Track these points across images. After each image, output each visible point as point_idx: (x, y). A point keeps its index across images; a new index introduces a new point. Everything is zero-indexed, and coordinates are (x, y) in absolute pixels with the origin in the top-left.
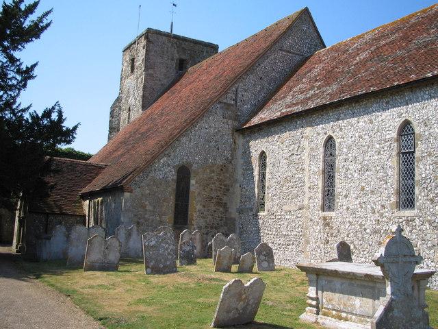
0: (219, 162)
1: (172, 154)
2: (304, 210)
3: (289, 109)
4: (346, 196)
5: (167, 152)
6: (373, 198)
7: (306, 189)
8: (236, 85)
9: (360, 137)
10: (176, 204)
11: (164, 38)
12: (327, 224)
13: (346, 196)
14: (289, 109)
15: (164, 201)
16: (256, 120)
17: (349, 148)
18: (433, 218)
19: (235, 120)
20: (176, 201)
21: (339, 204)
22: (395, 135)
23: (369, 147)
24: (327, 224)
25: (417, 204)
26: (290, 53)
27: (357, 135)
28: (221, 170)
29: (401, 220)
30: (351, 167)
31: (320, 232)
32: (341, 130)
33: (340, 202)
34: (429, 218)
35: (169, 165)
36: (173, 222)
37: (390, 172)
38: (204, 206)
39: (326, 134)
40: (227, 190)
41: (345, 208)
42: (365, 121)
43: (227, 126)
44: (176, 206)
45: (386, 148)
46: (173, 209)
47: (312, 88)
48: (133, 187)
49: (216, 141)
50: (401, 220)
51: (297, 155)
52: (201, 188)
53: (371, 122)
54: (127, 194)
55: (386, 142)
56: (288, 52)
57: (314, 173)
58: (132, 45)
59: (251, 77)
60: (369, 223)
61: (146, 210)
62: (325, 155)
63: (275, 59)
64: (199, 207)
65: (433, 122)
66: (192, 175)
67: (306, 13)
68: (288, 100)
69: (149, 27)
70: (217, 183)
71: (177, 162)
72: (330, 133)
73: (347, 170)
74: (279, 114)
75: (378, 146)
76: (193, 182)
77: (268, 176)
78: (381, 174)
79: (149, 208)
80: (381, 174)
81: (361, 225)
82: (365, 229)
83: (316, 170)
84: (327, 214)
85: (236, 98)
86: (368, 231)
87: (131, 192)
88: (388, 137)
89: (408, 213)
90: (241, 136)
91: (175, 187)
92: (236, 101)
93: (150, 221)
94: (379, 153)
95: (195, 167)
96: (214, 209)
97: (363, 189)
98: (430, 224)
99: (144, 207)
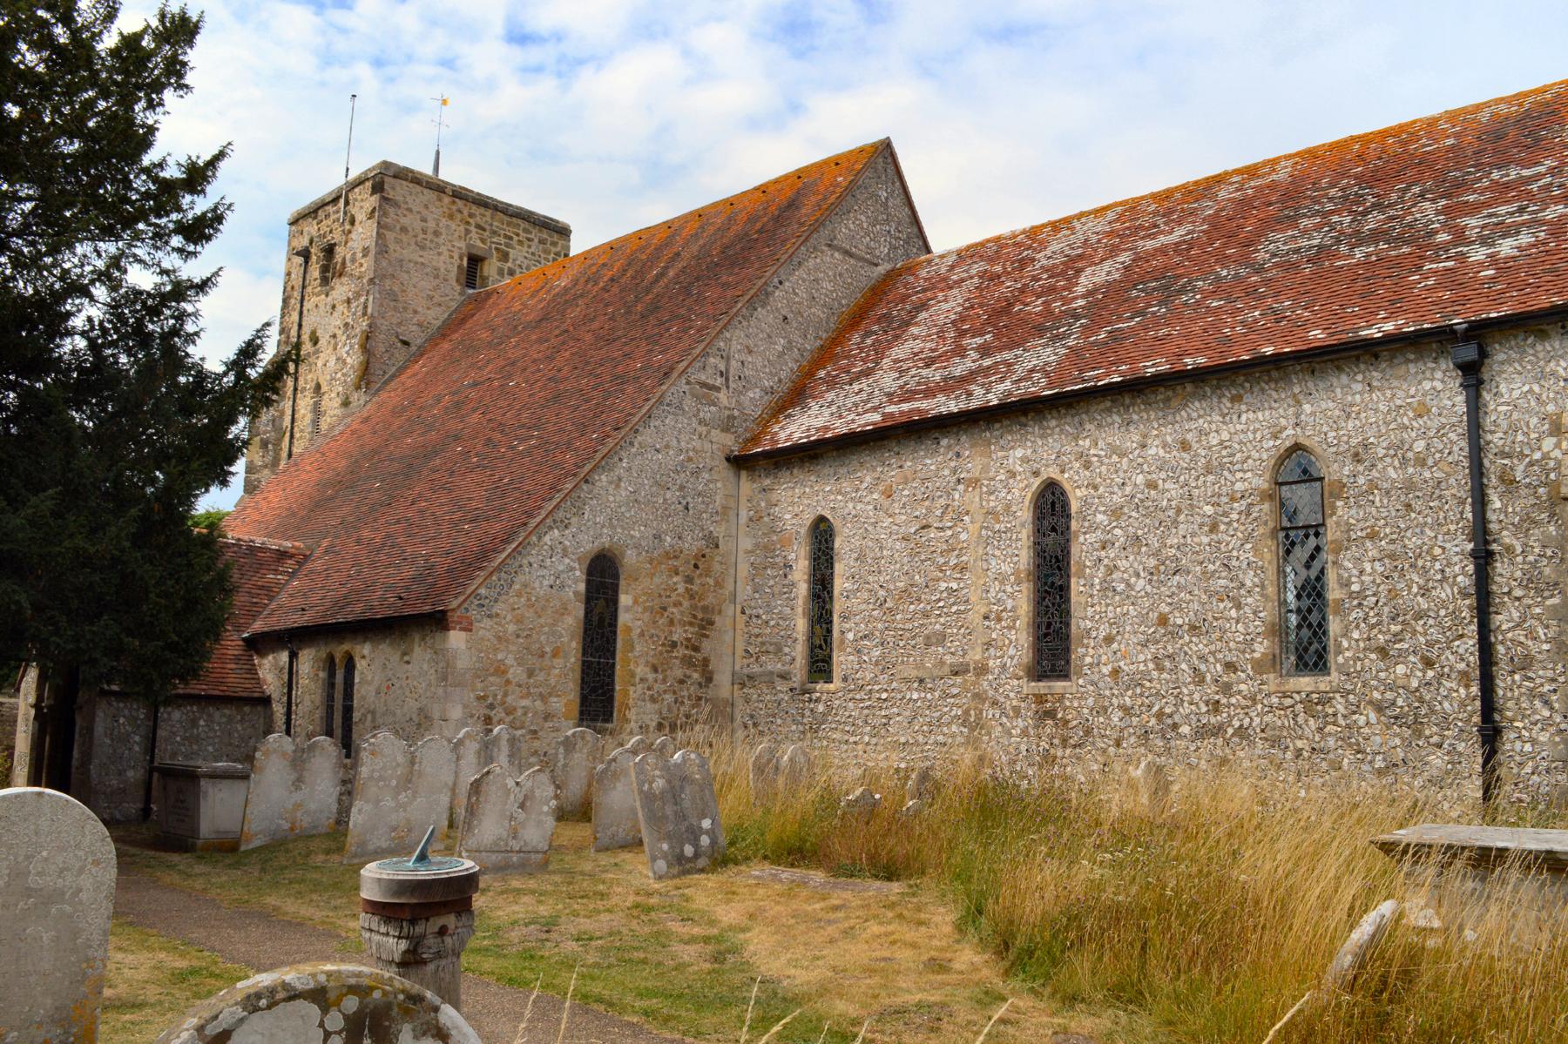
0: (691, 544)
1: (574, 520)
2: (970, 677)
3: (905, 407)
4: (1109, 640)
5: (560, 514)
6: (1200, 646)
7: (974, 618)
9: (1152, 485)
10: (584, 662)
12: (1051, 714)
13: (1109, 640)
14: (905, 407)
15: (555, 654)
16: (796, 429)
17: (1116, 513)
18: (1389, 695)
19: (726, 430)
20: (583, 655)
21: (1088, 660)
22: (1262, 483)
23: (1179, 511)
24: (1051, 714)
25: (1336, 660)
26: (851, 255)
27: (1140, 479)
28: (696, 566)
29: (1288, 702)
30: (1123, 564)
31: (1025, 733)
32: (1087, 465)
33: (1084, 654)
34: (1376, 695)
35: (565, 555)
37: (1249, 579)
38: (655, 670)
39: (1036, 474)
40: (705, 624)
41: (1106, 670)
42: (1165, 445)
43: (707, 446)
44: (586, 668)
45: (1235, 516)
46: (578, 675)
47: (960, 352)
48: (474, 613)
49: (682, 488)
50: (1288, 702)
51: (941, 529)
53: (1185, 446)
54: (456, 639)
55: (1233, 499)
57: (1002, 579)
58: (327, 204)
60: (1186, 709)
61: (508, 682)
62: (1039, 531)
63: (817, 269)
64: (641, 670)
65: (1381, 452)
66: (622, 583)
67: (884, 151)
68: (888, 380)
69: (389, 160)
70: (686, 604)
71: (588, 545)
72: (1053, 473)
73: (1111, 570)
74: (877, 417)
75: (1209, 510)
76: (625, 600)
77: (840, 584)
78: (1222, 582)
79: (516, 673)
80: (1222, 582)
81: (1160, 715)
82: (1175, 726)
83: (1006, 568)
84: (1042, 687)
86: (1185, 729)
88: (1239, 486)
89: (1305, 683)
90: (744, 474)
91: (579, 610)
92: (727, 379)
93: (519, 712)
94: (1214, 528)
95: (630, 558)
97: (1163, 620)
98: (1379, 708)
99: (500, 671)
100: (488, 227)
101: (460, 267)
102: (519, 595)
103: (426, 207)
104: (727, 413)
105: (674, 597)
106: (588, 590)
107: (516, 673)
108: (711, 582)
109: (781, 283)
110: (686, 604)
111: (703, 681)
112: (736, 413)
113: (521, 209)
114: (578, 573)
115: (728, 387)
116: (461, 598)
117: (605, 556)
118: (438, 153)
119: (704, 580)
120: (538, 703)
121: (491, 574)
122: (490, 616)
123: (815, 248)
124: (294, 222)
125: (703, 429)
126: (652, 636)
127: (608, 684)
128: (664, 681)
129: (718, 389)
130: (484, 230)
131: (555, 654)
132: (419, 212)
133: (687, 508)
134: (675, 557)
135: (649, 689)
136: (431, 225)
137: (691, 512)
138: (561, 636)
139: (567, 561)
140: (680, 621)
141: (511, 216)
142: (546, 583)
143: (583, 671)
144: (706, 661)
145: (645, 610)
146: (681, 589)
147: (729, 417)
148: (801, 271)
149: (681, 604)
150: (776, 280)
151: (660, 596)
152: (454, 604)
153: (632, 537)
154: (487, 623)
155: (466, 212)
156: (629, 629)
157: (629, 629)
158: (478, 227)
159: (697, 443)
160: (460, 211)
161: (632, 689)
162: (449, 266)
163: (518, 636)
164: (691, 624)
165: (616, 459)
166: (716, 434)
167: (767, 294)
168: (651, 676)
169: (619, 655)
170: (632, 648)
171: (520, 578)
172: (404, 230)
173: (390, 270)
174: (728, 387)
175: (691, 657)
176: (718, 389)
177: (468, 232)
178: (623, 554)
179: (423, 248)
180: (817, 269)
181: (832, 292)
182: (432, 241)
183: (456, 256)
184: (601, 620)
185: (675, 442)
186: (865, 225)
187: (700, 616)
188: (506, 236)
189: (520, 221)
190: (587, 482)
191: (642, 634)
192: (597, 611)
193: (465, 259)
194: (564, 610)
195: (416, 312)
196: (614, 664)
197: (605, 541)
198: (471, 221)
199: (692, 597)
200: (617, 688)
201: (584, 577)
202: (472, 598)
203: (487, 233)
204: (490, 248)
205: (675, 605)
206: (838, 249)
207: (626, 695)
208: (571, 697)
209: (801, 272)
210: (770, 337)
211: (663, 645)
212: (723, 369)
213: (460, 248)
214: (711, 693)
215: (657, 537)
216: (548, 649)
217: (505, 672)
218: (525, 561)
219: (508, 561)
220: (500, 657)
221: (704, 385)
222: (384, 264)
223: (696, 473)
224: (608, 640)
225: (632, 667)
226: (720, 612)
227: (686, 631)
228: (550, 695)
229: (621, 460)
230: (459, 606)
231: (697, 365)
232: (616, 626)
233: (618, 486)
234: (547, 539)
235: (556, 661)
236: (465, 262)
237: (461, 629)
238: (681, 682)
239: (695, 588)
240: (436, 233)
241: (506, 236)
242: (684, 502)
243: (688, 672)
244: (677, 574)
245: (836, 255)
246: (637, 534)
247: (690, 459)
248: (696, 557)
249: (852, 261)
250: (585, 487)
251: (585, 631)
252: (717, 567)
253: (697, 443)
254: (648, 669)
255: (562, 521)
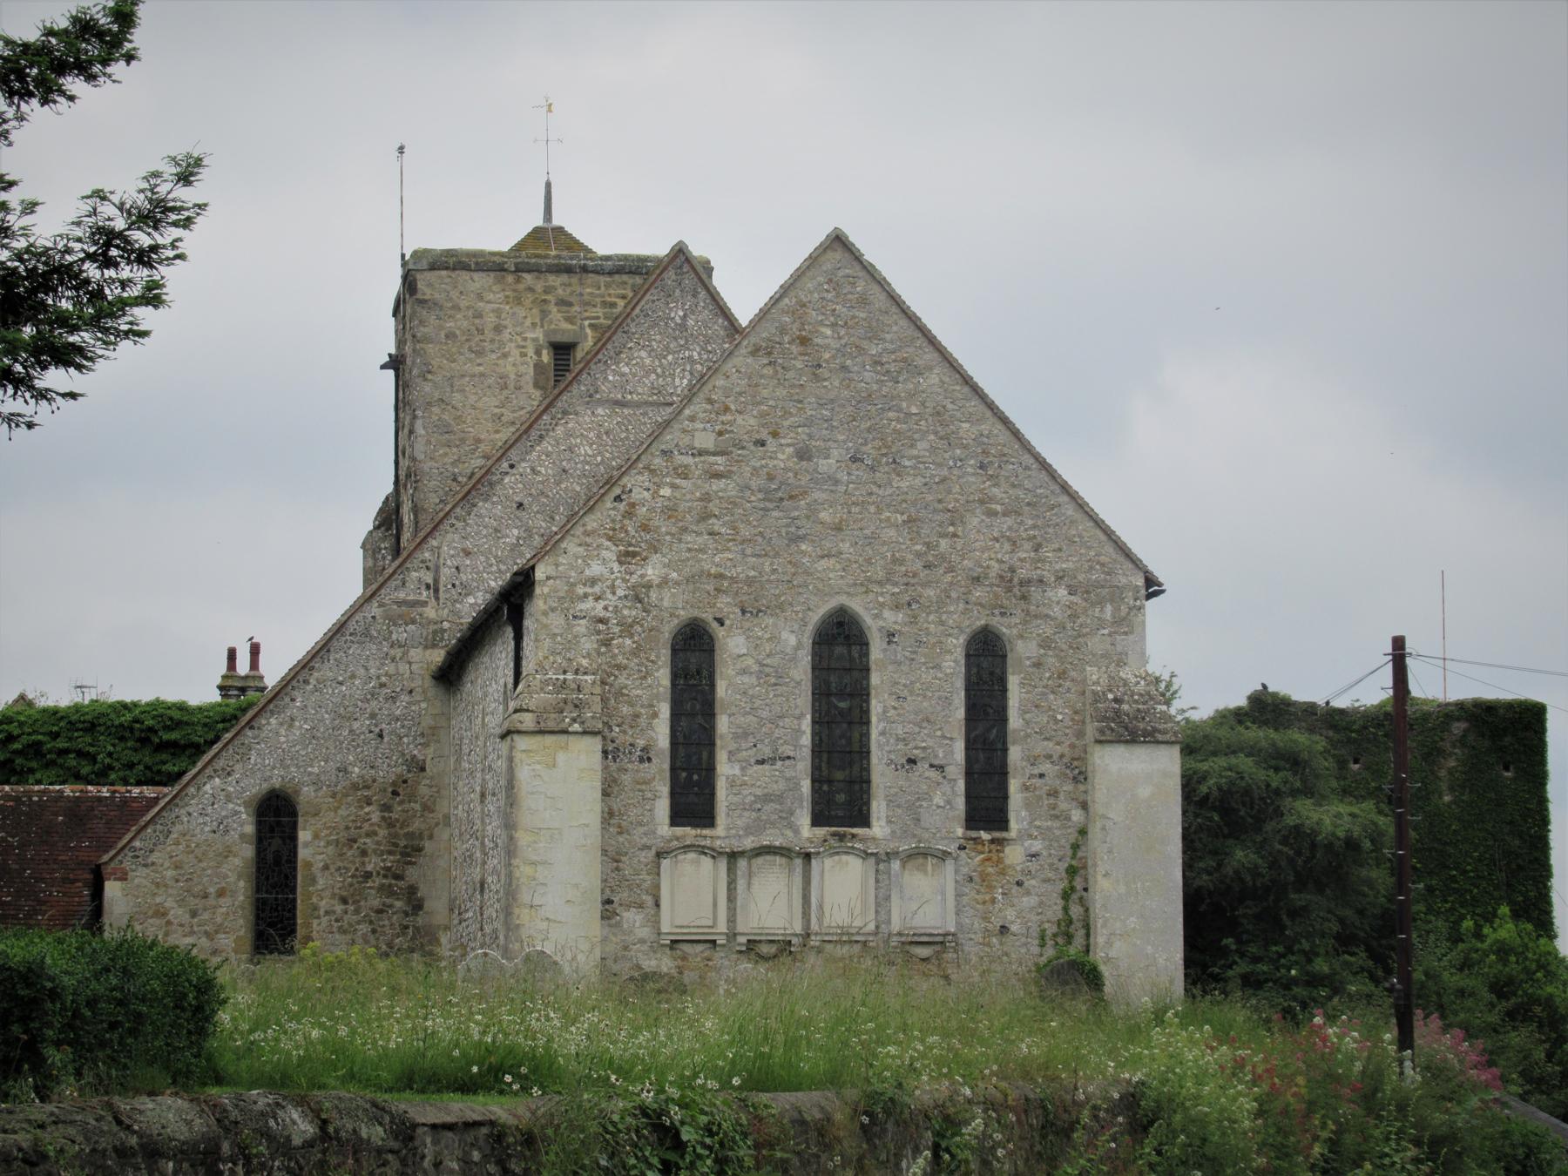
0: (387, 772)
1: (238, 767)
5: (220, 763)
8: (435, 543)
10: (258, 900)
11: (480, 280)
15: (221, 893)
20: (258, 890)
26: (622, 404)
28: (395, 793)
35: (229, 799)
36: (248, 945)
38: (344, 901)
43: (404, 668)
48: (127, 865)
49: (373, 716)
52: (331, 850)
56: (617, 403)
59: (483, 507)
61: (169, 923)
63: (569, 434)
66: (300, 820)
70: (382, 833)
71: (255, 787)
76: (304, 836)
79: (178, 913)
85: (436, 581)
87: (123, 878)
91: (249, 851)
92: (436, 591)
95: (307, 795)
96: (376, 903)
99: (161, 913)
100: (572, 299)
101: (538, 367)
102: (177, 843)
103: (480, 297)
104: (432, 627)
105: (366, 826)
106: (259, 831)
107: (178, 913)
108: (417, 807)
109: (512, 466)
110: (382, 833)
111: (409, 909)
112: (446, 625)
113: (626, 258)
114: (244, 816)
115: (437, 599)
116: (112, 853)
117: (278, 796)
118: (548, 185)
119: (406, 806)
120: (204, 939)
121: (145, 826)
122: (146, 866)
123: (565, 413)
124: (395, 314)
125: (398, 652)
126: (339, 869)
127: (288, 919)
128: (357, 912)
129: (424, 604)
130: (570, 304)
131: (221, 893)
132: (468, 308)
133: (381, 736)
134: (367, 787)
135: (337, 920)
136: (490, 319)
137: (386, 739)
138: (226, 876)
139: (231, 806)
140: (375, 851)
141: (610, 273)
142: (207, 829)
143: (258, 909)
144: (412, 890)
145: (328, 843)
146: (375, 817)
147: (435, 632)
148: (545, 444)
149: (375, 834)
150: (505, 465)
151: (347, 828)
152: (105, 858)
153: (310, 774)
154: (142, 871)
155: (539, 287)
156: (308, 865)
157: (308, 865)
158: (563, 303)
159: (391, 668)
160: (531, 289)
161: (315, 922)
162: (522, 369)
163: (177, 881)
164: (390, 853)
165: (287, 699)
166: (415, 654)
167: (491, 484)
168: (339, 908)
169: (299, 890)
170: (313, 881)
171: (178, 828)
172: (450, 336)
173: (437, 395)
174: (437, 599)
175: (390, 885)
176: (424, 604)
177: (544, 314)
178: (297, 792)
179: (480, 353)
180: (569, 434)
181: (594, 456)
182: (492, 341)
183: (531, 352)
184: (277, 862)
185: (362, 671)
186: (648, 361)
187: (402, 843)
188: (604, 304)
189: (625, 278)
190: (252, 728)
191: (326, 867)
192: (273, 848)
193: (545, 352)
194: (228, 852)
195: (478, 441)
196: (295, 900)
197: (276, 783)
198: (549, 297)
199: (391, 824)
200: (299, 921)
201: (252, 819)
202: (126, 851)
203: (576, 308)
204: (582, 328)
205: (368, 835)
206: (601, 402)
207: (308, 925)
208: (242, 933)
209: (546, 445)
210: (496, 530)
211: (353, 876)
212: (430, 581)
213: (535, 340)
214: (420, 920)
215: (343, 770)
216: (212, 890)
217: (164, 914)
218: (183, 811)
219: (164, 814)
220: (158, 900)
221: (400, 603)
222: (427, 389)
223: (393, 699)
224: (286, 877)
225: (314, 900)
226: (431, 837)
227: (384, 861)
228: (217, 932)
229: (293, 700)
230: (112, 859)
231: (393, 584)
232: (295, 862)
233: (291, 726)
234: (208, 787)
235: (222, 901)
236: (546, 357)
237: (115, 879)
238: (380, 911)
239: (394, 816)
240: (498, 329)
241: (604, 304)
242: (377, 730)
243: (388, 901)
244: (369, 804)
245: (600, 411)
246: (316, 770)
247: (383, 685)
248: (394, 784)
249: (626, 411)
250: (249, 733)
251: (259, 869)
252: (423, 790)
253: (391, 668)
254: (336, 902)
255: (223, 769)
